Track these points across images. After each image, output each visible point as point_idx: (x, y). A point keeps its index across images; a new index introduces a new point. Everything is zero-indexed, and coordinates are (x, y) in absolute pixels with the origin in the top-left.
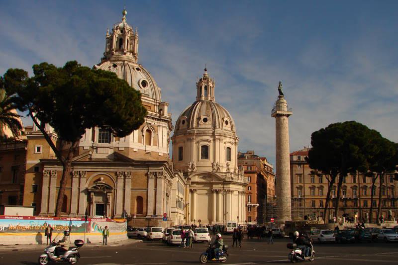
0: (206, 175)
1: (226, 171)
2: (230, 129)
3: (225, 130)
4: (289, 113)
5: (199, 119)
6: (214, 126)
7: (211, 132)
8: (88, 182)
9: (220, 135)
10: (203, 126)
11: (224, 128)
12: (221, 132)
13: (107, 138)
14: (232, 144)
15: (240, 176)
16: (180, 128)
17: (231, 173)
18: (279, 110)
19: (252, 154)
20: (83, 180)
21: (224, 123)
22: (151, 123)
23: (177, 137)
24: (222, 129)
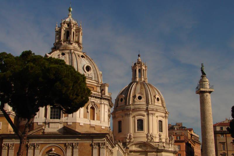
0: (142, 145)
1: (158, 141)
2: (161, 105)
3: (157, 106)
4: (211, 90)
5: (134, 97)
6: (147, 103)
7: (145, 108)
8: (41, 153)
9: (153, 110)
10: (139, 103)
11: (156, 104)
12: (153, 108)
13: (57, 115)
14: (163, 118)
15: (170, 145)
16: (119, 105)
17: (163, 143)
18: (202, 88)
19: (181, 126)
20: (37, 151)
21: (156, 100)
22: (94, 101)
23: (116, 112)
24: (154, 105)
